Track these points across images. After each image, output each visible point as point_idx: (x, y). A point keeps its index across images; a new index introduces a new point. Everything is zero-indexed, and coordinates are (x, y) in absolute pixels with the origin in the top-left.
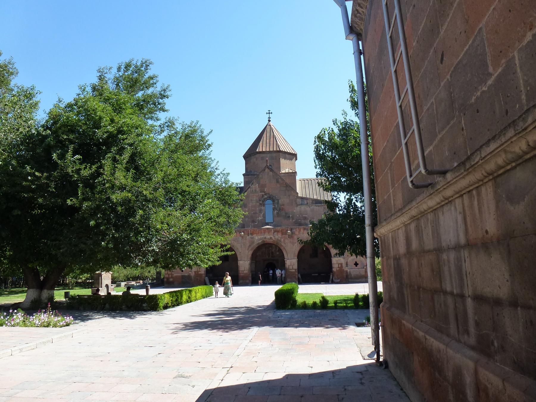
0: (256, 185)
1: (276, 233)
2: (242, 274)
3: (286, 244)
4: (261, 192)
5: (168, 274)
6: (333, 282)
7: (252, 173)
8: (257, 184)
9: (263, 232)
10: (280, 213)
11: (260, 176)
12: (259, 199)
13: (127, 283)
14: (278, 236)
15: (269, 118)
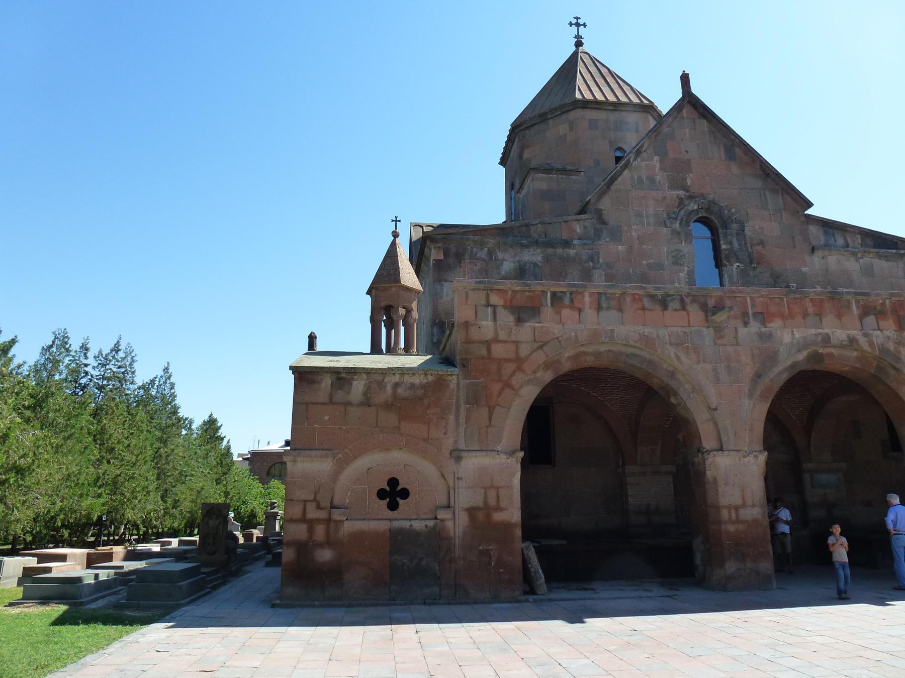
0: (652, 160)
1: (871, 320)
2: (731, 528)
5: (303, 520)
8: (656, 158)
9: (811, 310)
10: (751, 273)
12: (668, 214)
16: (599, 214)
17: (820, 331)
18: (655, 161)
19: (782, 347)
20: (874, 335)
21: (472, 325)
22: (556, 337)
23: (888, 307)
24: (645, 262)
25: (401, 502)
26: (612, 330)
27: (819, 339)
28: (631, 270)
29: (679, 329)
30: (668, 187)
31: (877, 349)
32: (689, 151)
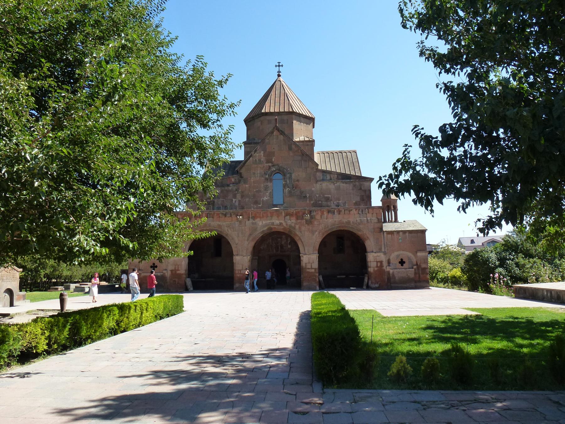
0: (260, 153)
1: (288, 217)
2: (238, 275)
4: (268, 162)
6: (369, 288)
7: (255, 141)
8: (262, 152)
9: (269, 215)
10: (293, 192)
11: (267, 141)
13: (80, 284)
14: (291, 221)
15: (279, 72)
16: (241, 173)
25: (155, 269)
27: (271, 223)
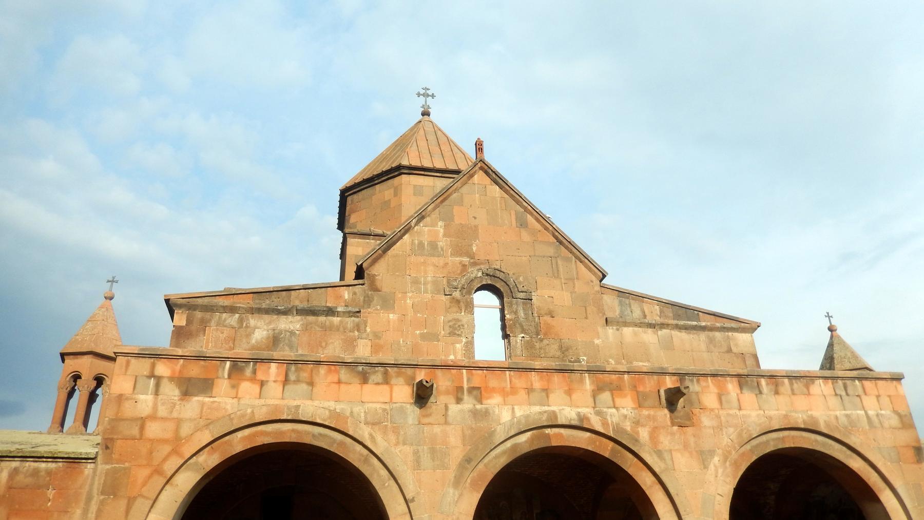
1: (606, 396)
3: (667, 456)
4: (459, 251)
8: (440, 223)
10: (537, 345)
16: (373, 278)
17: (546, 408)
18: (439, 227)
19: (500, 426)
20: (609, 414)
21: (127, 399)
22: (227, 414)
23: (626, 381)
24: (418, 332)
26: (298, 406)
27: (545, 417)
28: (401, 342)
29: (378, 406)
30: (451, 254)
31: (611, 429)
32: (477, 217)
